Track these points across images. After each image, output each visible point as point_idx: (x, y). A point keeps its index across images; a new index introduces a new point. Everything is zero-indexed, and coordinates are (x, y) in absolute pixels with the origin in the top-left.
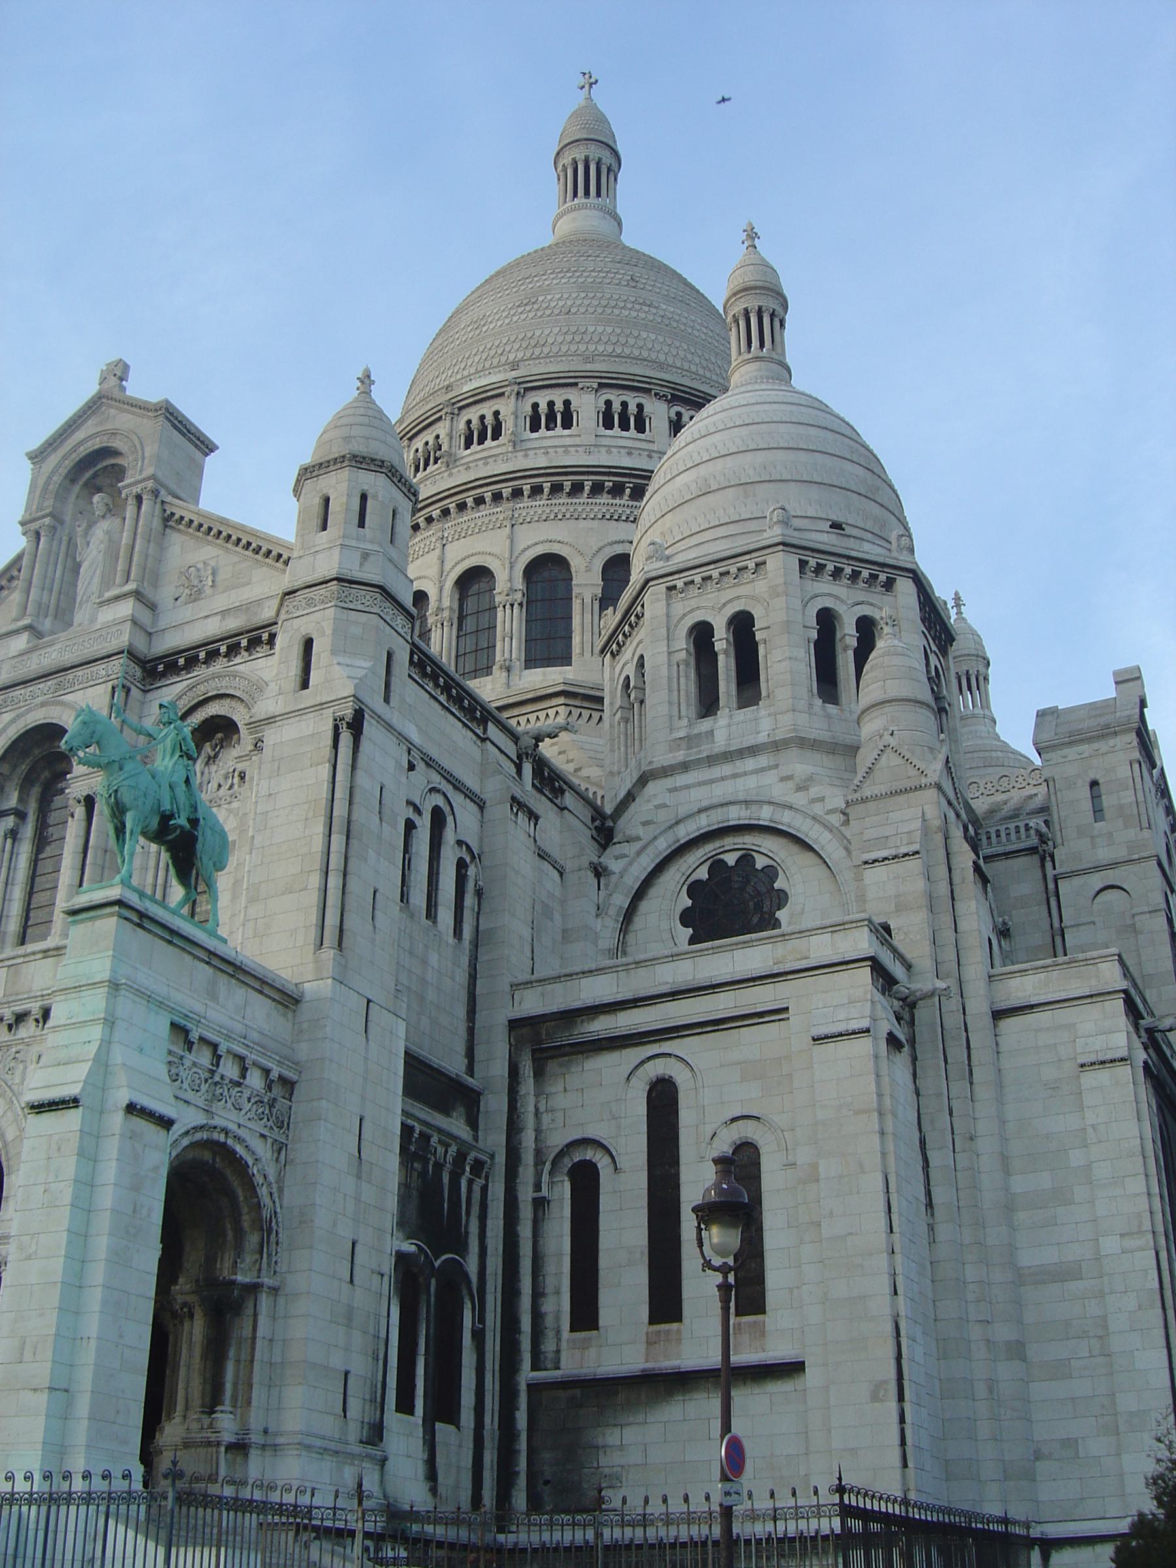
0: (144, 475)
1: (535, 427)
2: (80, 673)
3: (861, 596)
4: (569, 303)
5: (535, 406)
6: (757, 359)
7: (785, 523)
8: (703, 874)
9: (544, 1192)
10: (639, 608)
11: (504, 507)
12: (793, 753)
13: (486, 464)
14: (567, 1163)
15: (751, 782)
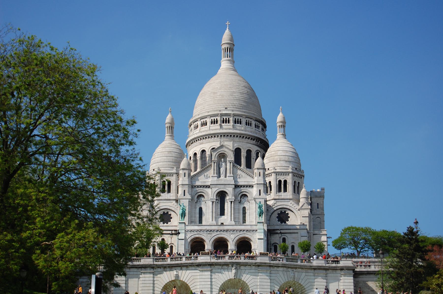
0: (232, 160)
1: (235, 123)
2: (228, 186)
3: (298, 179)
4: (239, 97)
5: (235, 119)
6: (283, 134)
7: (292, 169)
8: (279, 212)
9: (271, 248)
10: (271, 175)
11: (232, 138)
12: (292, 201)
13: (229, 130)
14: (274, 245)
15: (287, 203)
